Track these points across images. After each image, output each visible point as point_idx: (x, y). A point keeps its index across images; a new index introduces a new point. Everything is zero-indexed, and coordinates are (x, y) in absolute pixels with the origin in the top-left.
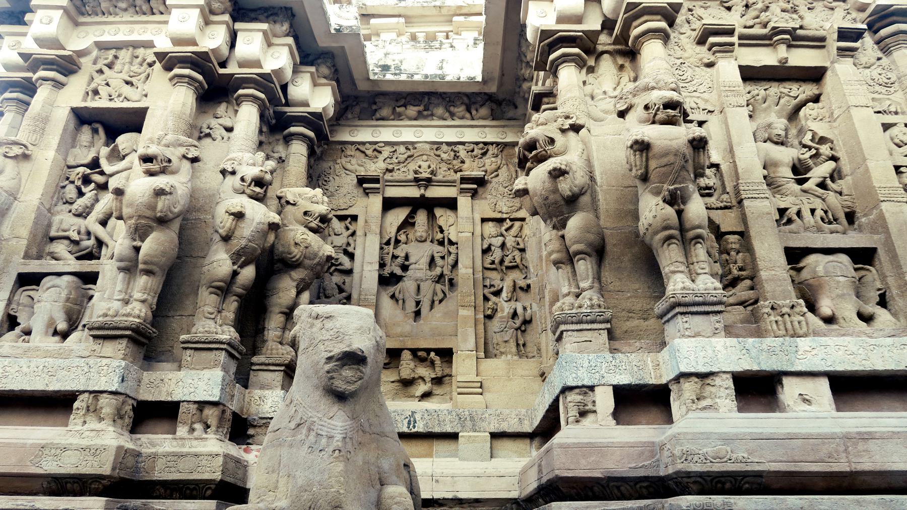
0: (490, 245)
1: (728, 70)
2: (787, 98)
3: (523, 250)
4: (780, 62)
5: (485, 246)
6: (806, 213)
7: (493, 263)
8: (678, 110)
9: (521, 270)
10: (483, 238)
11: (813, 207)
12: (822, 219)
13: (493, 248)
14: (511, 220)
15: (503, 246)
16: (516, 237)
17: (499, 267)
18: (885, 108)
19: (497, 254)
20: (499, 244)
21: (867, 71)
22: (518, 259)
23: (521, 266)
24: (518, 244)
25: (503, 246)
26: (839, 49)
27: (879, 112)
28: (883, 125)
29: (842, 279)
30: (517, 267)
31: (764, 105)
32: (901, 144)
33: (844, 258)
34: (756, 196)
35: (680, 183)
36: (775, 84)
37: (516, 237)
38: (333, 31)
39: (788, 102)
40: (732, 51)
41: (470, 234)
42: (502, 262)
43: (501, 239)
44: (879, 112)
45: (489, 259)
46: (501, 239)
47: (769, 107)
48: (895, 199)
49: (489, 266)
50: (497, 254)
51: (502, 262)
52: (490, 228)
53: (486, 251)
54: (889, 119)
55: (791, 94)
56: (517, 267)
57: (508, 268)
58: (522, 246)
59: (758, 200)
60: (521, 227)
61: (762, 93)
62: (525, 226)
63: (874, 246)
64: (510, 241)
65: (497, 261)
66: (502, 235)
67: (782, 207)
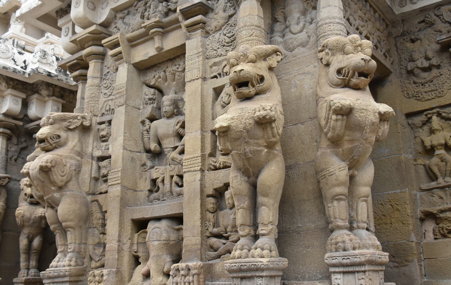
1: (123, 73)
2: (177, 73)
4: (158, 51)
6: (167, 181)
8: (46, 142)
11: (171, 174)
12: (177, 184)
18: (220, 71)
21: (217, 35)
26: (188, 27)
27: (215, 77)
28: (215, 89)
29: (156, 243)
31: (166, 84)
32: (225, 105)
33: (164, 224)
34: (114, 182)
35: (48, 195)
36: (169, 64)
38: (27, 76)
39: (179, 76)
40: (122, 58)
44: (215, 77)
47: (169, 84)
48: (192, 169)
54: (219, 82)
55: (180, 70)
59: (115, 186)
61: (162, 74)
63: (181, 212)
67: (154, 178)
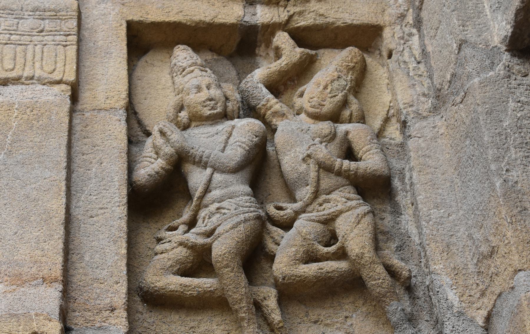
0: (179, 164)
3: (376, 189)
5: (151, 166)
7: (200, 262)
9: (377, 305)
10: (137, 130)
13: (197, 178)
14: (300, 37)
15: (258, 166)
16: (335, 117)
17: (229, 280)
19: (224, 213)
20: (235, 153)
22: (354, 231)
23: (377, 278)
24: (349, 153)
25: (258, 166)
30: (350, 286)
37: (335, 117)
41: (59, 95)
42: (254, 256)
43: (245, 129)
45: (172, 243)
46: (245, 129)
49: (174, 282)
50: (224, 213)
51: (254, 256)
52: (182, 78)
53: (154, 200)
56: (350, 286)
57: (292, 294)
58: (371, 161)
60: (359, 80)
62: (379, 71)
64: (298, 142)
65: (222, 248)
66: (250, 110)
